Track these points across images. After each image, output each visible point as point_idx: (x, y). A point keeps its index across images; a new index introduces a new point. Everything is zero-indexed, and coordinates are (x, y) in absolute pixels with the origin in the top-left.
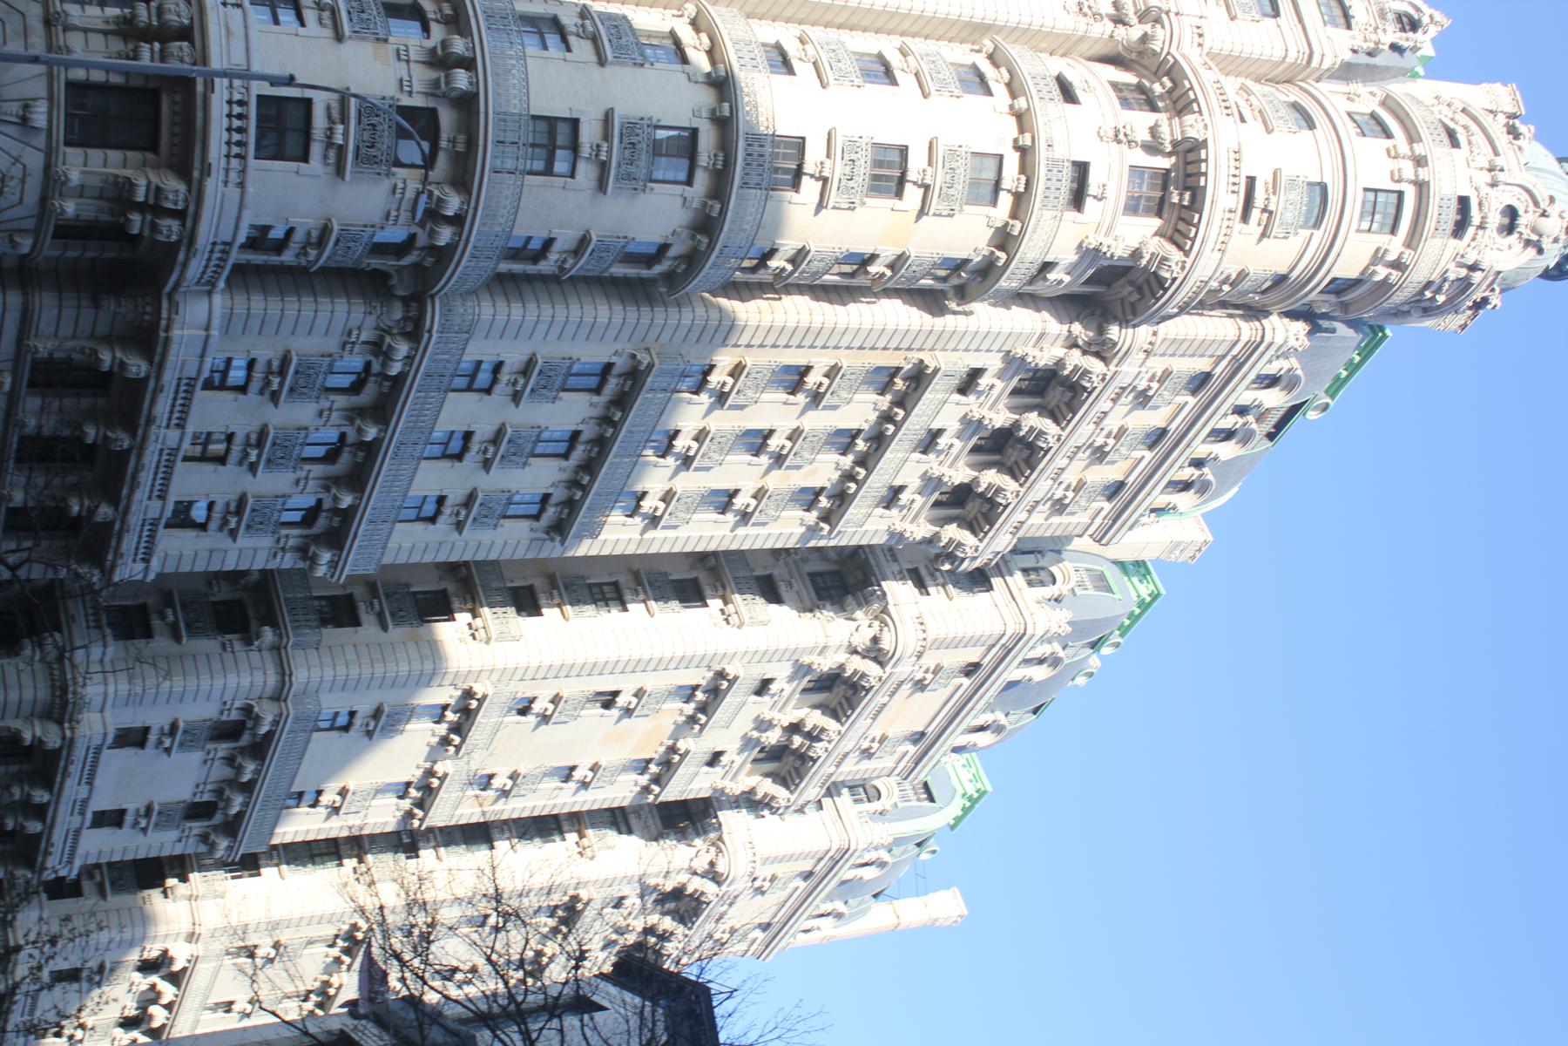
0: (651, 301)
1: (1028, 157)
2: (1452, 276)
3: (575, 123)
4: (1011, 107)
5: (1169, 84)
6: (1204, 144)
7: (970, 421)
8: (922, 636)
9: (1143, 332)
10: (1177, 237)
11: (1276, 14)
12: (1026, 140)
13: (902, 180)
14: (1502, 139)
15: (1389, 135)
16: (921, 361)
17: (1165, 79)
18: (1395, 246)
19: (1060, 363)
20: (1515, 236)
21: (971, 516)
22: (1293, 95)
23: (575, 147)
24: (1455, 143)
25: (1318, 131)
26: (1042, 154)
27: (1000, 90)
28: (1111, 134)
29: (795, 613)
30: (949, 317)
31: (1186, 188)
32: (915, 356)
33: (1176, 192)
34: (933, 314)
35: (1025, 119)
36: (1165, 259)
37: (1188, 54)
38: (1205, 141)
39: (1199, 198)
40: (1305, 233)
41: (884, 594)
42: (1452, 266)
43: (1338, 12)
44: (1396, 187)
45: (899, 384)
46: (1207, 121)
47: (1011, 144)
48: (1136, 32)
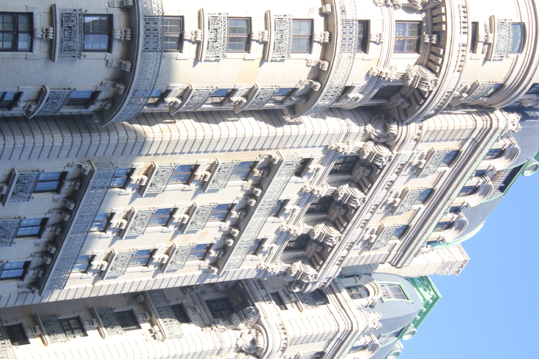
0: (89, 130)
1: (330, 20)
3: (30, 16)
7: (282, 233)
8: (284, 337)
9: (413, 127)
10: (431, 65)
13: (249, 40)
16: (270, 156)
19: (361, 151)
21: (310, 256)
23: (31, 31)
26: (339, 17)
29: (199, 328)
30: (286, 127)
31: (434, 33)
34: (275, 126)
39: (442, 38)
40: (514, 56)
41: (257, 311)
45: (257, 172)
47: (318, 11)
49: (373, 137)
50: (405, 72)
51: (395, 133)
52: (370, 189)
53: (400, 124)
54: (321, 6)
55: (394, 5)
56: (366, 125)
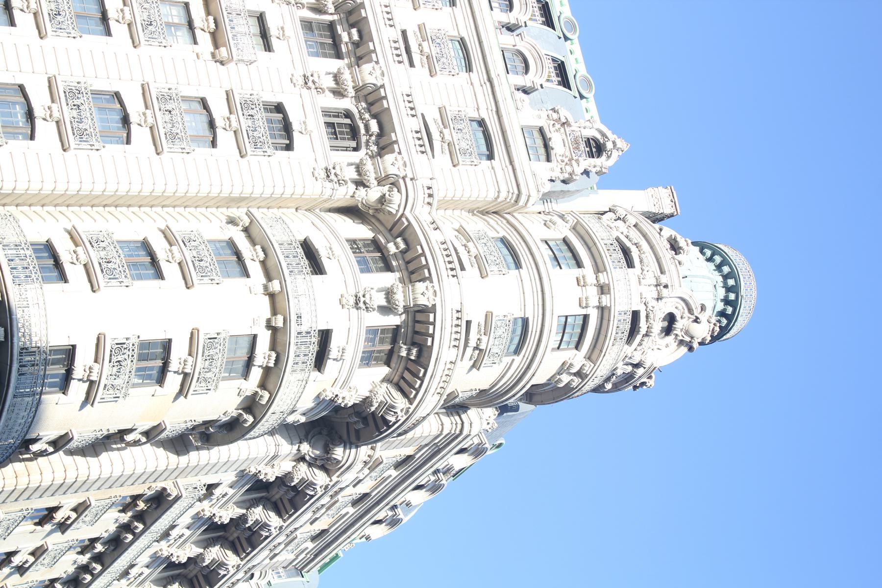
1: (280, 336)
2: (619, 372)
4: (266, 287)
5: (402, 246)
6: (433, 309)
9: (364, 451)
11: (491, 157)
12: (279, 322)
13: (163, 371)
14: (666, 254)
15: (579, 265)
16: (164, 489)
17: (399, 240)
18: (578, 359)
19: (288, 476)
20: (671, 338)
21: (192, 575)
22: (503, 231)
24: (630, 264)
25: (524, 271)
26: (294, 328)
27: (255, 268)
28: (352, 301)
30: (193, 454)
31: (414, 344)
32: (158, 486)
33: (406, 346)
34: (178, 453)
35: (278, 299)
36: (393, 407)
37: (419, 215)
38: (434, 306)
39: (425, 354)
40: (507, 360)
42: (620, 364)
43: (539, 142)
44: (584, 312)
45: (141, 505)
46: (437, 288)
48: (373, 194)
49: (307, 458)
50: (368, 394)
51: (340, 458)
52: (291, 516)
53: (348, 446)
54: (269, 316)
55: (367, 308)
56: (301, 443)
